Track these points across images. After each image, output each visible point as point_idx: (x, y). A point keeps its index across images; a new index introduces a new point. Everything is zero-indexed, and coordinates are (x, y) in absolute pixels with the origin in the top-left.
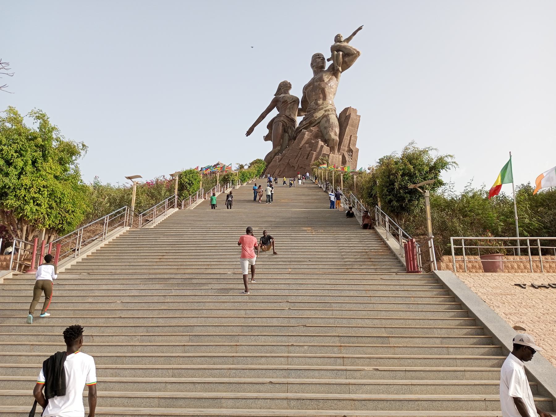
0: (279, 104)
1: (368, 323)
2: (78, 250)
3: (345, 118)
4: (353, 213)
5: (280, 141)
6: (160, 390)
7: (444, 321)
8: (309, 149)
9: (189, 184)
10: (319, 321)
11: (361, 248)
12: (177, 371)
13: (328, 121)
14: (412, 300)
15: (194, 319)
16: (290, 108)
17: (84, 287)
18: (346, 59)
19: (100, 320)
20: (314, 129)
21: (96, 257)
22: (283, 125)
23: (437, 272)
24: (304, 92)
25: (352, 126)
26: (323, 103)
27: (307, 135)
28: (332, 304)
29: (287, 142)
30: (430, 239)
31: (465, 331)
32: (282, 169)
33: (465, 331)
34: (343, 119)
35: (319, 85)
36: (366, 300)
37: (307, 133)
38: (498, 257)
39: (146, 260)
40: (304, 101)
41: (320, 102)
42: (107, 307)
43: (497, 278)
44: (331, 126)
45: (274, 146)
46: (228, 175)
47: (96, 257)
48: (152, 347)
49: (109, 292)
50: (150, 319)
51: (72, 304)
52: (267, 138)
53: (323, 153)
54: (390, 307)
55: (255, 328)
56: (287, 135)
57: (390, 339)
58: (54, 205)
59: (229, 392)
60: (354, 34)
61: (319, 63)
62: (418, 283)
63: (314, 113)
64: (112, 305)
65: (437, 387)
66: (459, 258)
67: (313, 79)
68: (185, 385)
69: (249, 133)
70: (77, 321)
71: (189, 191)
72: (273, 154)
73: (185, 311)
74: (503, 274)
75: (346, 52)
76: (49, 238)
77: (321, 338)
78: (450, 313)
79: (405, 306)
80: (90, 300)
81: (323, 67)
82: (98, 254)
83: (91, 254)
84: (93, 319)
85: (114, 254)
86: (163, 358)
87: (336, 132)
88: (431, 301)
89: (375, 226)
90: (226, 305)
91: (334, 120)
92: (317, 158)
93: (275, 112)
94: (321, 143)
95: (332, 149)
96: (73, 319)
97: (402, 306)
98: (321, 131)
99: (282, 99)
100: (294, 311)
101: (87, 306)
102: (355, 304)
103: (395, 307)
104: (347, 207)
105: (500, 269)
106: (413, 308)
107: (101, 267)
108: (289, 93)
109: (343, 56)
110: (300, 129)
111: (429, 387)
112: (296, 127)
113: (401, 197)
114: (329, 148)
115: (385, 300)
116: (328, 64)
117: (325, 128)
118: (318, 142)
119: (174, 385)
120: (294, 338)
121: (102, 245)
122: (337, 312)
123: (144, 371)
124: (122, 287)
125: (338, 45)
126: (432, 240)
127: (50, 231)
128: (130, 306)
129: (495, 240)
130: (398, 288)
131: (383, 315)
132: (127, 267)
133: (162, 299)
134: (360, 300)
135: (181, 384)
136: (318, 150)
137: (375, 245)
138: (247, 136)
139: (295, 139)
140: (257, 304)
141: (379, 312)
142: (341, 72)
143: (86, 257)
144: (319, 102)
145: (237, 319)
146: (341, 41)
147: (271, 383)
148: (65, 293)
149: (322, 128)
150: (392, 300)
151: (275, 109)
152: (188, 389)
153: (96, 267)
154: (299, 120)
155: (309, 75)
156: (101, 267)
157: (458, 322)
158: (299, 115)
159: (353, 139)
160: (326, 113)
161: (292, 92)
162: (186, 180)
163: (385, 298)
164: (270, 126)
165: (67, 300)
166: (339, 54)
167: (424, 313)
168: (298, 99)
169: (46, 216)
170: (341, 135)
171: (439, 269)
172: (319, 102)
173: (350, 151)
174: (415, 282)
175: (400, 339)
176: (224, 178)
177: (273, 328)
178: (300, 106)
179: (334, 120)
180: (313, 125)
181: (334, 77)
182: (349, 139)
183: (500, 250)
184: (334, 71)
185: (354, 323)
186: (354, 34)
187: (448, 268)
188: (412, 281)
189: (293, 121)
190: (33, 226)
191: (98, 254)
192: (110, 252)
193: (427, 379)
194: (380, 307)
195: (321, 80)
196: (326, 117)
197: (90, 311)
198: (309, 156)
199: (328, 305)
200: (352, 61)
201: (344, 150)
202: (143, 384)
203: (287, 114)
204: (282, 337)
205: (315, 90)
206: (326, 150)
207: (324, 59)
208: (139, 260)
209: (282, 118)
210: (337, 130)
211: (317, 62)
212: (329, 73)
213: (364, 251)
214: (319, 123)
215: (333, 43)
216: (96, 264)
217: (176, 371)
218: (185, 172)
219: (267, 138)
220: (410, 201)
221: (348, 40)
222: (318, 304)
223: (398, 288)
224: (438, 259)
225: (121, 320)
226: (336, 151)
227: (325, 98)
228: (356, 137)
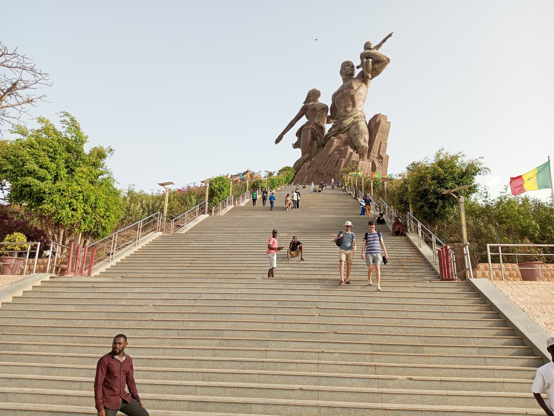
0: (308, 113)
1: (402, 331)
2: (112, 254)
3: (375, 125)
4: (383, 220)
5: (309, 148)
6: (190, 394)
7: (481, 331)
8: (338, 156)
9: (219, 190)
10: (350, 328)
11: (393, 255)
12: (207, 374)
13: (358, 127)
14: (447, 309)
15: (224, 323)
16: (319, 116)
17: (118, 290)
18: (376, 66)
19: (133, 322)
20: (343, 136)
21: (130, 261)
22: (312, 133)
23: (473, 280)
24: (333, 100)
25: (382, 133)
26: (352, 110)
27: (336, 142)
28: (363, 311)
29: (316, 149)
30: (465, 246)
31: (503, 341)
32: (311, 176)
33: (503, 341)
34: (373, 126)
35: (349, 92)
36: (398, 308)
37: (336, 140)
38: (537, 265)
39: (177, 265)
40: (333, 108)
41: (349, 109)
42: (139, 309)
43: (536, 286)
44: (360, 133)
45: (303, 154)
46: (257, 182)
47: (130, 261)
48: (182, 350)
49: (142, 295)
50: (181, 322)
51: (105, 307)
52: (296, 146)
53: (352, 159)
54: (424, 315)
55: (285, 333)
56: (316, 142)
57: (424, 347)
58: (90, 210)
59: (258, 397)
60: (384, 41)
61: (348, 70)
62: (453, 291)
63: (343, 120)
64: (144, 308)
65: (474, 398)
66: (496, 265)
67: (342, 87)
68: (215, 389)
69: (277, 141)
70: (110, 324)
71: (219, 197)
72: (302, 162)
73: (215, 315)
74: (542, 283)
75: (376, 59)
76: (85, 242)
77: (353, 345)
78: (487, 322)
79: (439, 314)
80: (123, 303)
81: (352, 74)
82: (132, 259)
83: (124, 258)
84: (125, 322)
85: (148, 259)
86: (193, 361)
88: (467, 309)
89: (406, 233)
90: (255, 309)
91: (363, 127)
92: (345, 166)
93: (304, 120)
94: (350, 150)
95: (361, 156)
96: (106, 321)
97: (436, 314)
99: (310, 107)
100: (324, 318)
101: (120, 309)
102: (387, 312)
103: (430, 316)
104: (378, 213)
105: (539, 277)
106: (447, 316)
107: (134, 271)
108: (318, 101)
110: (328, 136)
111: (466, 398)
112: (325, 135)
113: (433, 203)
114: (358, 155)
115: (418, 308)
116: (357, 72)
117: (355, 135)
118: (347, 149)
119: (204, 388)
120: (324, 344)
121: (136, 249)
122: (369, 320)
123: (174, 373)
124: (154, 290)
125: (368, 53)
126: (467, 247)
127: (86, 235)
128: (162, 309)
129: (534, 247)
130: (432, 296)
131: (417, 323)
132: (159, 271)
133: (192, 303)
134: (392, 307)
135: (211, 388)
136: (347, 157)
137: (406, 252)
138: (276, 144)
139: (324, 146)
140: (287, 309)
141: (413, 320)
142: (371, 79)
143: (120, 261)
145: (267, 324)
146: (371, 49)
147: (301, 389)
148: (99, 296)
149: (351, 135)
150: (426, 308)
151: (304, 117)
152: (218, 392)
153: (130, 271)
154: (328, 127)
155: (338, 82)
156: (134, 271)
157: (495, 332)
158: (328, 122)
159: (383, 145)
160: (356, 120)
161: (321, 100)
162: (216, 186)
163: (419, 306)
164: (299, 134)
165: (101, 302)
166: (369, 61)
167: (460, 322)
169: (82, 221)
170: (371, 142)
171: (475, 277)
173: (380, 157)
174: (450, 289)
175: (435, 348)
176: (254, 184)
177: (303, 334)
178: (329, 114)
179: (363, 127)
180: (343, 132)
181: (363, 84)
182: (379, 145)
183: (539, 258)
184: (364, 78)
185: (386, 331)
186: (384, 41)
187: (484, 276)
188: (447, 289)
189: (322, 128)
190: (70, 230)
191: (132, 259)
192: (142, 256)
193: (463, 390)
194: (413, 315)
195: (351, 87)
197: (123, 314)
198: (338, 162)
199: (359, 312)
200: (382, 68)
201: (374, 157)
202: (174, 387)
203: (316, 121)
204: (312, 344)
205: (344, 98)
206: (355, 157)
207: (353, 66)
208: (170, 265)
209: (311, 126)
210: (367, 137)
211: (347, 70)
212: (358, 80)
213: (395, 258)
214: (348, 130)
215: (362, 50)
216: (129, 268)
217: (206, 375)
218: (215, 179)
219: (296, 146)
220: (443, 207)
221: (378, 47)
222: (348, 311)
223: (432, 296)
224: (474, 267)
225: (152, 322)
226: (366, 158)
227: (354, 105)
228: (386, 144)
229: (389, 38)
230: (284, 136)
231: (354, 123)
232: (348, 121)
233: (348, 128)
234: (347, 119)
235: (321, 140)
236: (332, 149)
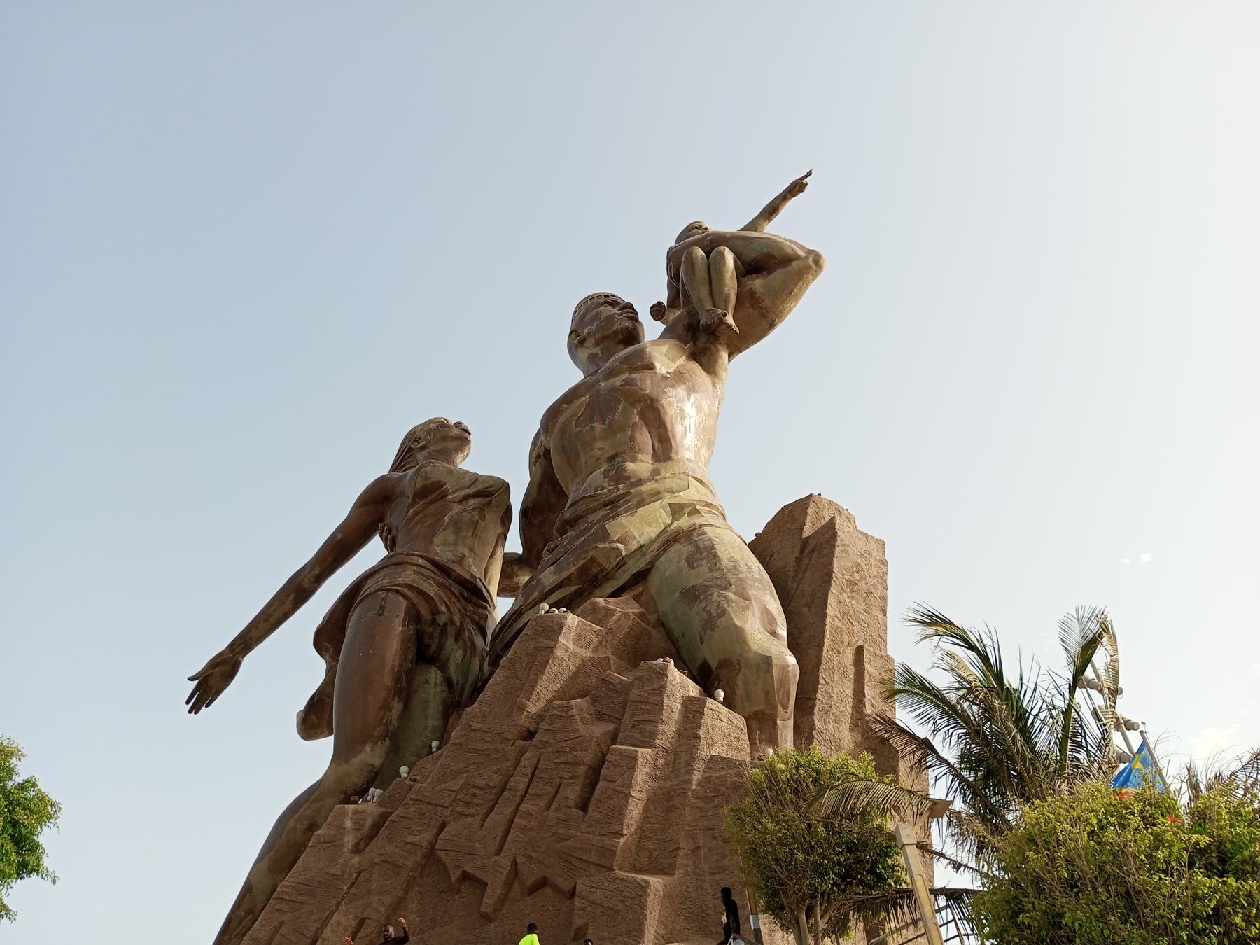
0: (395, 518)
3: (802, 551)
5: (386, 706)
8: (600, 730)
13: (705, 553)
16: (456, 525)
18: (757, 283)
22: (414, 617)
26: (656, 472)
29: (434, 721)
37: (572, 620)
41: (641, 466)
44: (723, 580)
52: (313, 720)
53: (704, 752)
56: (434, 675)
60: (771, 211)
61: (610, 319)
75: (751, 254)
81: (631, 336)
87: (766, 612)
94: (680, 684)
95: (761, 725)
98: (662, 624)
109: (732, 289)
114: (739, 720)
117: (693, 595)
118: (662, 674)
138: (195, 709)
144: (630, 466)
149: (665, 605)
160: (684, 522)
166: (722, 255)
168: (504, 488)
170: (805, 637)
172: (630, 466)
178: (514, 544)
181: (695, 366)
182: (851, 670)
186: (771, 211)
189: (475, 595)
196: (687, 542)
198: (597, 780)
206: (723, 730)
211: (603, 330)
212: (673, 342)
214: (641, 577)
227: (664, 448)
229: (792, 203)
230: (248, 662)
231: (670, 540)
232: (640, 528)
233: (642, 564)
234: (631, 510)
235: (465, 669)
236: (547, 686)
